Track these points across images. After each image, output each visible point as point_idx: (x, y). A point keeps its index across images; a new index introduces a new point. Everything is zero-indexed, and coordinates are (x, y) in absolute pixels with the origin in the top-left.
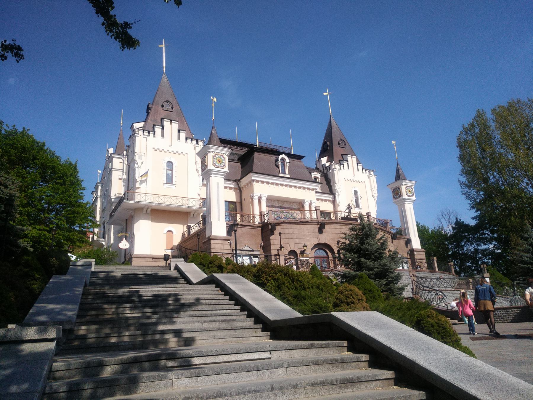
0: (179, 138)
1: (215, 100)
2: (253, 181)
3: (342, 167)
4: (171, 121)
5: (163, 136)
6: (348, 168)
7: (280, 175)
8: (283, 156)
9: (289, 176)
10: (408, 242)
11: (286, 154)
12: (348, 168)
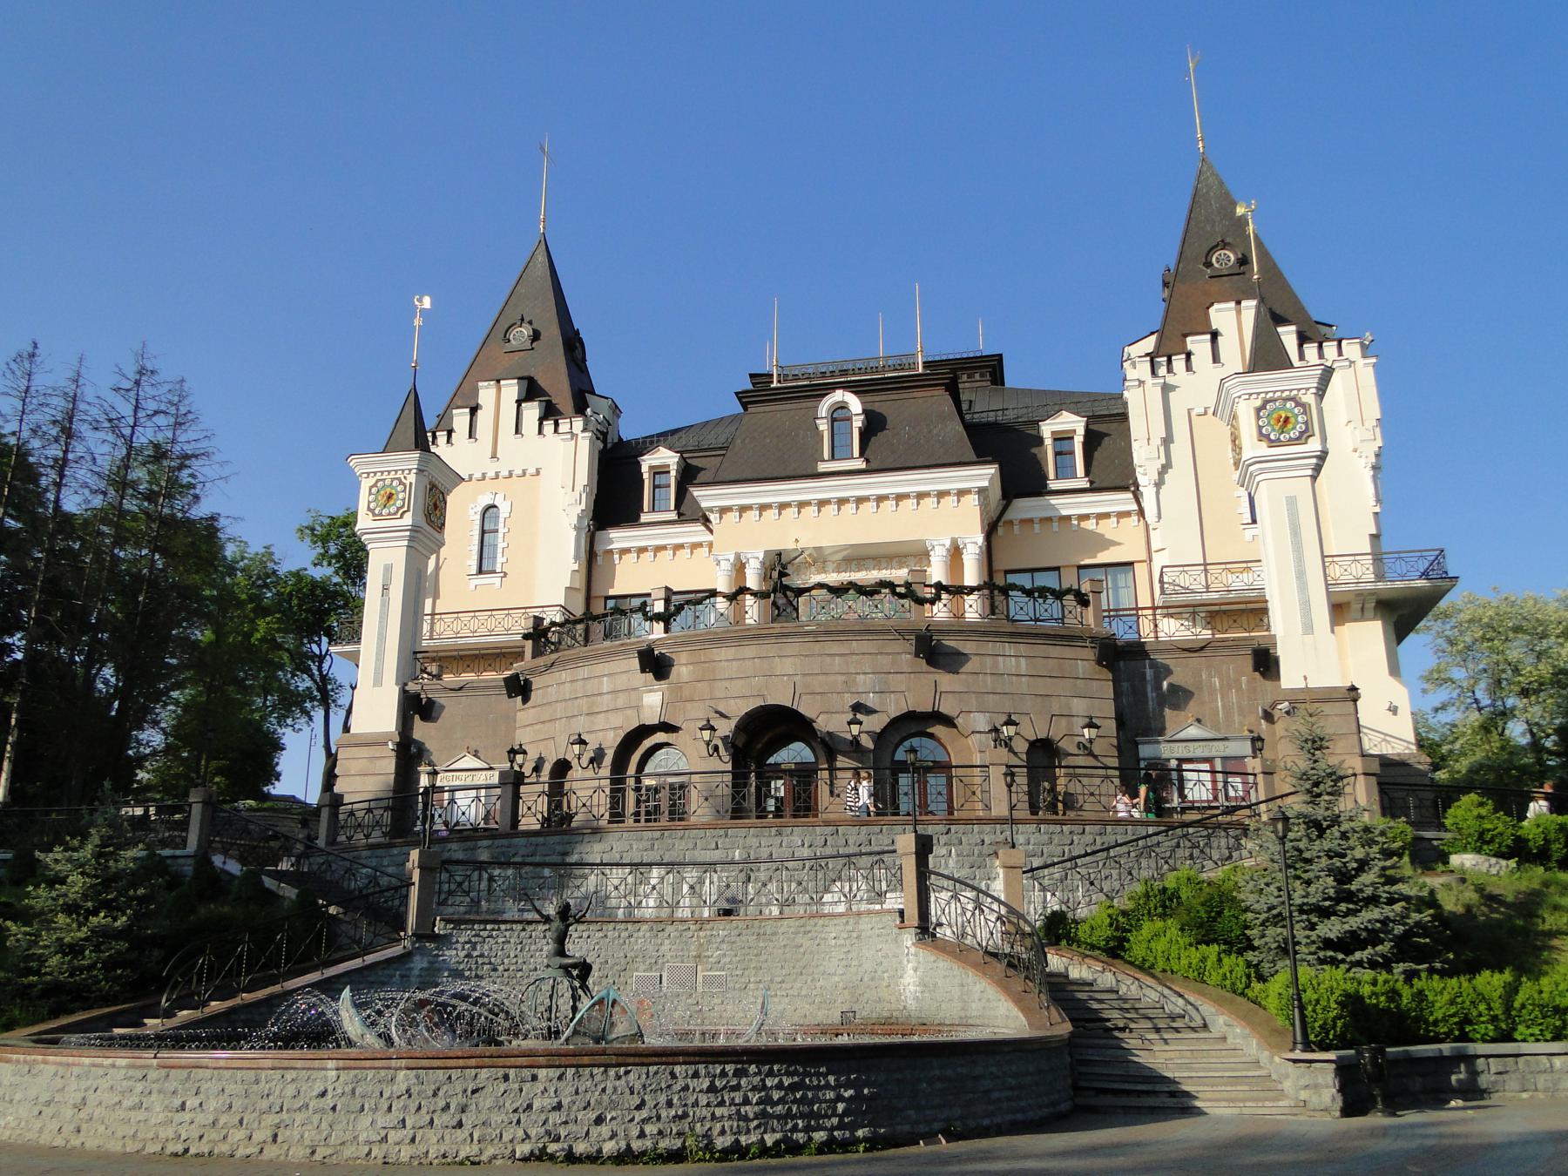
1: (427, 302)
2: (711, 510)
6: (1216, 358)
7: (823, 467)
8: (838, 396)
10: (1266, 662)
11: (846, 386)
12: (1216, 358)
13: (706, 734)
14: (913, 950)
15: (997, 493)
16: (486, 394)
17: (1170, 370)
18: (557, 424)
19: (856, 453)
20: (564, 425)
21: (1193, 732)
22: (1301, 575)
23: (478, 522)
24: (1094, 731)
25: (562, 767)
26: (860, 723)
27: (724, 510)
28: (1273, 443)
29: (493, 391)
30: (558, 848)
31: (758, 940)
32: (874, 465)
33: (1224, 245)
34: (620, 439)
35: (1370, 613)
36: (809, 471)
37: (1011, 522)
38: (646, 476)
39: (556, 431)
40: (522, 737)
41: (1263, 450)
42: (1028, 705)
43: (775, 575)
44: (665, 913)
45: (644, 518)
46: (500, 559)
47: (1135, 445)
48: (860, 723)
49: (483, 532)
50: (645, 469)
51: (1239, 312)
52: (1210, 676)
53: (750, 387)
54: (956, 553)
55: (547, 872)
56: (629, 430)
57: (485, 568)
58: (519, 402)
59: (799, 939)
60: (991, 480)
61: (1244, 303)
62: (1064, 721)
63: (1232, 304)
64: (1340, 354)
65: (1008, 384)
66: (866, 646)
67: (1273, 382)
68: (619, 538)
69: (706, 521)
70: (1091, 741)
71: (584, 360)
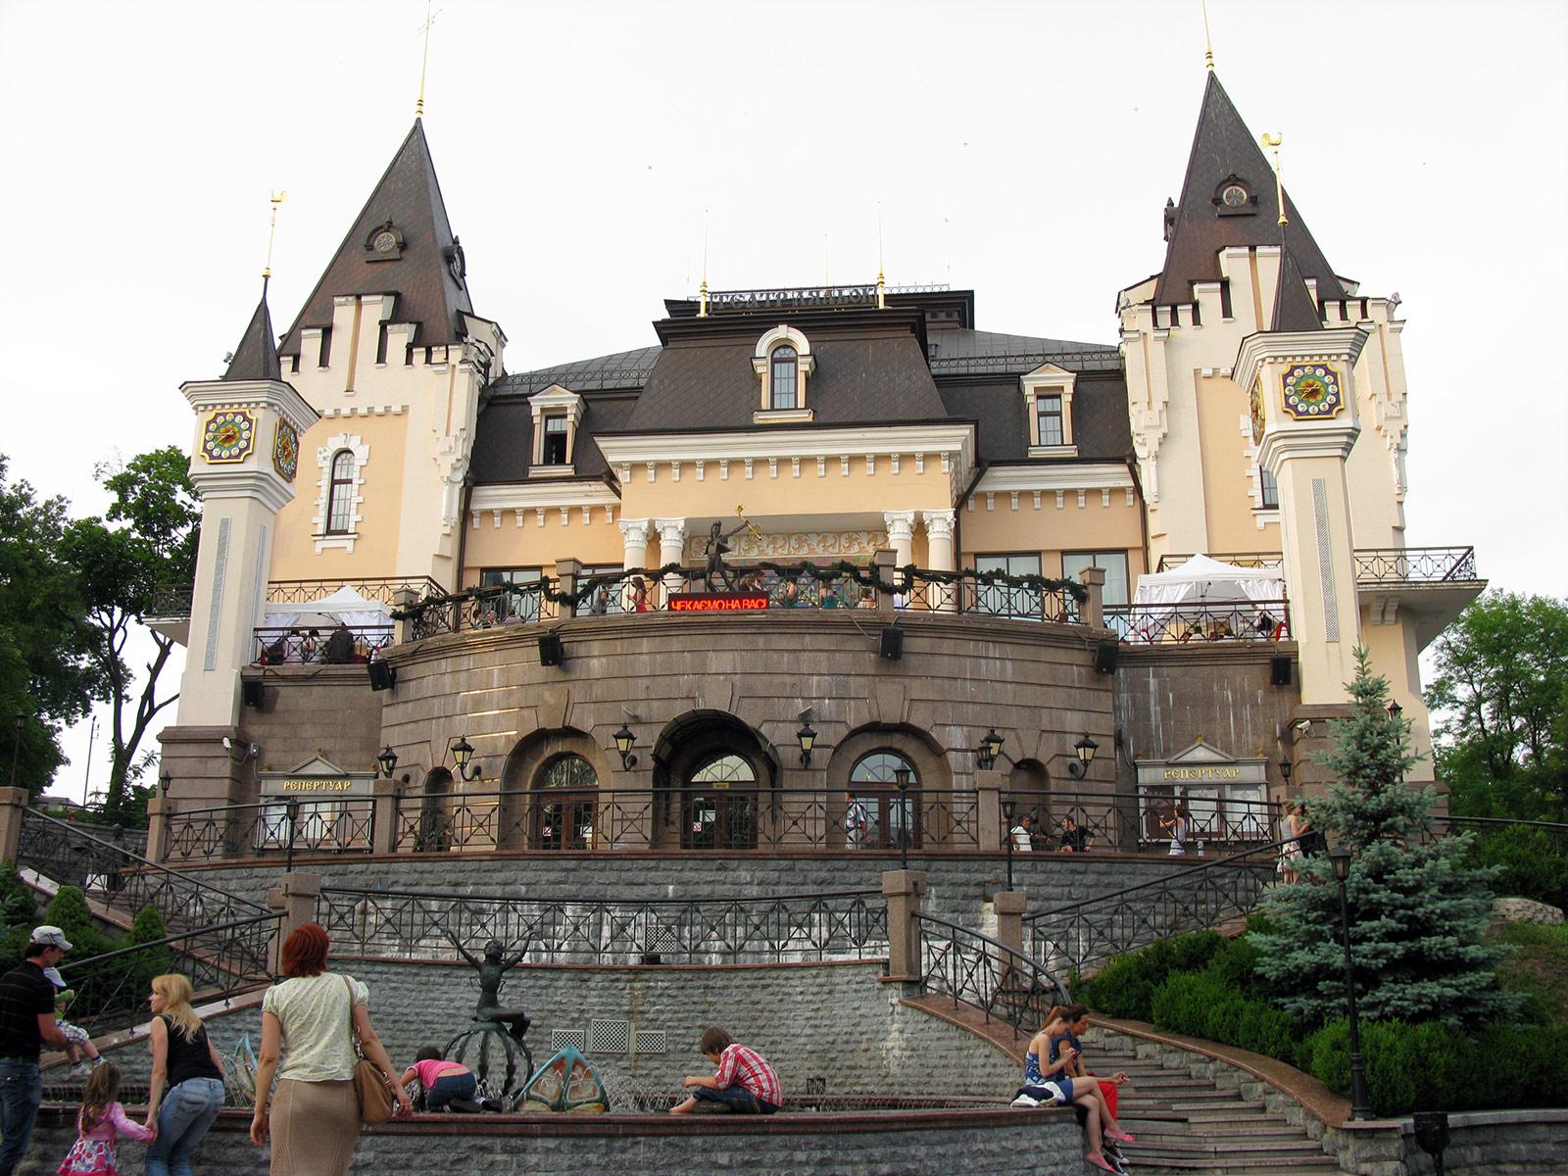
0: (381, 357)
2: (620, 465)
3: (1185, 314)
4: (359, 297)
5: (324, 361)
6: (1227, 312)
7: (759, 419)
8: (782, 331)
9: (806, 417)
10: (1284, 671)
11: (794, 322)
12: (1227, 312)
13: (623, 744)
14: (899, 1009)
15: (969, 459)
16: (343, 314)
17: (1175, 322)
18: (429, 353)
19: (801, 403)
20: (438, 355)
21: (1200, 754)
22: (1326, 572)
23: (327, 471)
24: (1090, 751)
25: (440, 778)
26: (814, 735)
27: (636, 467)
28: (1301, 416)
29: (351, 309)
30: (449, 877)
31: (705, 994)
32: (822, 419)
33: (1233, 180)
34: (504, 373)
35: (1390, 617)
36: (743, 422)
37: (984, 496)
38: (536, 420)
39: (428, 361)
40: (390, 738)
41: (1290, 424)
42: (1012, 718)
43: (713, 549)
44: (581, 958)
45: (534, 473)
46: (354, 518)
47: (1132, 410)
48: (814, 735)
49: (334, 482)
50: (536, 411)
51: (1253, 259)
52: (1222, 688)
53: (667, 316)
54: (920, 530)
55: (434, 905)
56: (516, 361)
57: (333, 528)
58: (383, 325)
59: (757, 995)
60: (964, 444)
61: (1259, 250)
62: (1054, 738)
63: (1246, 250)
64: (1364, 315)
65: (978, 327)
66: (824, 642)
67: (1303, 346)
68: (495, 497)
69: (610, 479)
70: (1086, 763)
71: (463, 274)
